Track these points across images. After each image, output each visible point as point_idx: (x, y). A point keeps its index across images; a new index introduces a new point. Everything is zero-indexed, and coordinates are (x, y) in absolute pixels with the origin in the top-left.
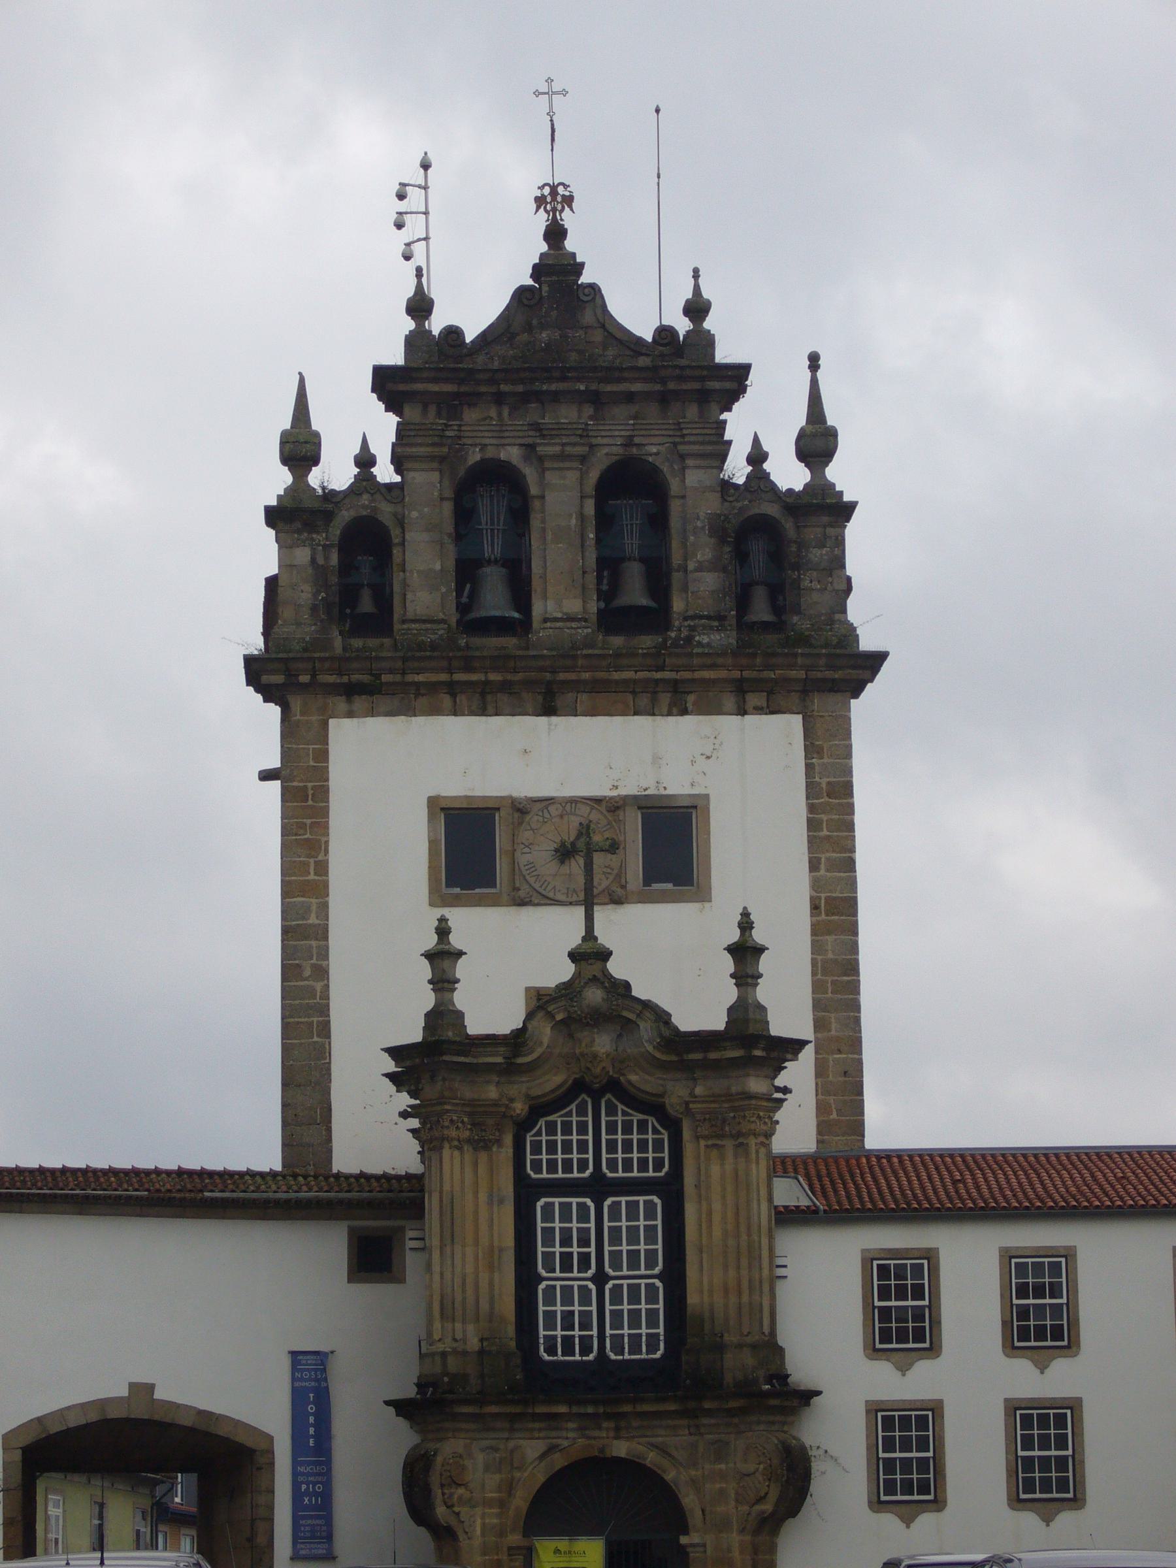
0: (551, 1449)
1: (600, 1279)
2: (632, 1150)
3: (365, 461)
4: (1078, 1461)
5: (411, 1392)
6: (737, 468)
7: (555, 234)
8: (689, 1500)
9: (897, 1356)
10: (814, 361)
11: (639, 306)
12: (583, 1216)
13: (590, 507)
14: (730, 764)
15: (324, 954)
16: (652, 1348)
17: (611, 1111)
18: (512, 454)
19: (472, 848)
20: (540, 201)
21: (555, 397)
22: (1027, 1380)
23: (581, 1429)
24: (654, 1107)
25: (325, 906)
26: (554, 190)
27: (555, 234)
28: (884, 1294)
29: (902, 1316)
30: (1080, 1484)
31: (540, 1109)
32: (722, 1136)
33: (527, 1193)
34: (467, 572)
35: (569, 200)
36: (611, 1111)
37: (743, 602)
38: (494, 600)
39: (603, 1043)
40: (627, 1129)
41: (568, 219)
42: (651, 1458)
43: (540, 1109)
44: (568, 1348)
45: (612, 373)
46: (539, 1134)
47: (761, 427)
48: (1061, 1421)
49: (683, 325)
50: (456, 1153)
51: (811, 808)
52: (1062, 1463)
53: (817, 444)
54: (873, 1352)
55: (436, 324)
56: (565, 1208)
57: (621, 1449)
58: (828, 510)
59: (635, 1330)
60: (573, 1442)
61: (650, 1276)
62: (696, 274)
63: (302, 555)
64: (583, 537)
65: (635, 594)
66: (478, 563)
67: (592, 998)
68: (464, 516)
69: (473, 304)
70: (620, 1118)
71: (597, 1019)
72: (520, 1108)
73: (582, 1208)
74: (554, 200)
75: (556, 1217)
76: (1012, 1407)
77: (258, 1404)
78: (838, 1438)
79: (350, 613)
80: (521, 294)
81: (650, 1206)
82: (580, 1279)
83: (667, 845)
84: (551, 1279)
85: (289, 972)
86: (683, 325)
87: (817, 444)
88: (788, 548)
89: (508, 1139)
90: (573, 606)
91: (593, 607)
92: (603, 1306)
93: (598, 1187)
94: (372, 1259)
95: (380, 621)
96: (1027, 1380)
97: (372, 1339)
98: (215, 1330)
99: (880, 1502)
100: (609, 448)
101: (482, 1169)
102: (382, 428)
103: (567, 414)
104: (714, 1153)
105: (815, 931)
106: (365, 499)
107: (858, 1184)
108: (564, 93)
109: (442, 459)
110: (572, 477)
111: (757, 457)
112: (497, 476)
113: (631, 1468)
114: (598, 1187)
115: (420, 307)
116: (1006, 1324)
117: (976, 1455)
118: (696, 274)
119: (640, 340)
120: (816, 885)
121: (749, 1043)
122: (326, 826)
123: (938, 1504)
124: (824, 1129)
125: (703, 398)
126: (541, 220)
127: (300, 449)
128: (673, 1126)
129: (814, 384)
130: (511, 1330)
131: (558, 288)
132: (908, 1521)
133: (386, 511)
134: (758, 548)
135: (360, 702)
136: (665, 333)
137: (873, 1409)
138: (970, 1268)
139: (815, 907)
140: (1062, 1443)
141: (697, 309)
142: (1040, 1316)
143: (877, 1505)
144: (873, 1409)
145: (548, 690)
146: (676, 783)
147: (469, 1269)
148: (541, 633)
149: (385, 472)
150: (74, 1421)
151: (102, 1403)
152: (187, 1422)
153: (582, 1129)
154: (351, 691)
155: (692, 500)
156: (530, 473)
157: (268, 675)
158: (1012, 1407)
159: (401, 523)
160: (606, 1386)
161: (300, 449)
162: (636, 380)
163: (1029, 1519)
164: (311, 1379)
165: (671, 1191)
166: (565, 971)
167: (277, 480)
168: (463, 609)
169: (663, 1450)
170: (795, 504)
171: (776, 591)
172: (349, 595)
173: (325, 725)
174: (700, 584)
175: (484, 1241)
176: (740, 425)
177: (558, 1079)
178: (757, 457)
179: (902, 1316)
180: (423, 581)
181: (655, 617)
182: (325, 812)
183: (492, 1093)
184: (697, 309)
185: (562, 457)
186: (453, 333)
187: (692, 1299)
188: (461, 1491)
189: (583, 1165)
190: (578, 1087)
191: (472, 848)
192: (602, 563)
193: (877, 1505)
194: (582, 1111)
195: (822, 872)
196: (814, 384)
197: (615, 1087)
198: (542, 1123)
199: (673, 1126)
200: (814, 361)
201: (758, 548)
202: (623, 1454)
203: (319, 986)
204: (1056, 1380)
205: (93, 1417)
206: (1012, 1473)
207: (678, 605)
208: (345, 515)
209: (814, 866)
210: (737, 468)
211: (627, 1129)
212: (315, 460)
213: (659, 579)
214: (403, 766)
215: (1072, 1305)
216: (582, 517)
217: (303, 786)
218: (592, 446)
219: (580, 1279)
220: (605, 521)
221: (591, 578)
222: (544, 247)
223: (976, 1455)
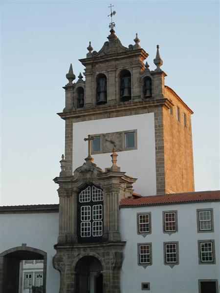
0: (79, 254)
3: (81, 77)
7: (112, 31)
9: (143, 234)
10: (158, 47)
12: (89, 210)
14: (142, 123)
16: (100, 234)
17: (94, 189)
18: (103, 72)
19: (96, 142)
20: (110, 26)
23: (84, 250)
25: (72, 157)
26: (112, 23)
27: (112, 31)
28: (141, 222)
29: (144, 226)
32: (109, 192)
33: (79, 205)
35: (114, 25)
36: (94, 189)
39: (88, 176)
40: (96, 192)
41: (114, 29)
42: (97, 256)
43: (81, 189)
45: (118, 54)
46: (81, 194)
48: (174, 246)
49: (134, 44)
50: (63, 199)
51: (156, 130)
52: (175, 255)
53: (158, 62)
54: (139, 233)
55: (92, 52)
56: (86, 208)
57: (91, 254)
58: (160, 73)
60: (83, 254)
62: (137, 34)
63: (69, 95)
64: (116, 86)
69: (97, 48)
70: (95, 190)
71: (87, 171)
73: (89, 208)
74: (112, 25)
75: (87, 210)
76: (165, 244)
79: (80, 103)
84: (84, 222)
86: (134, 44)
90: (114, 98)
91: (118, 97)
93: (91, 204)
95: (82, 105)
99: (201, 262)
100: (120, 68)
101: (68, 200)
104: (108, 195)
105: (156, 153)
106: (80, 84)
108: (113, 6)
109: (92, 74)
110: (114, 74)
112: (102, 77)
113: (93, 258)
115: (90, 49)
116: (164, 227)
117: (158, 254)
118: (137, 34)
119: (126, 48)
120: (156, 145)
122: (72, 143)
123: (151, 264)
124: (158, 191)
126: (110, 29)
127: (71, 76)
129: (158, 50)
132: (145, 268)
136: (130, 46)
137: (139, 245)
138: (157, 215)
139: (156, 149)
140: (174, 251)
141: (137, 41)
142: (170, 224)
143: (139, 264)
144: (139, 245)
145: (108, 113)
146: (130, 128)
147: (66, 220)
149: (84, 79)
150: (12, 251)
152: (31, 250)
153: (89, 193)
155: (135, 75)
156: (106, 75)
158: (165, 244)
159: (85, 86)
162: (123, 55)
163: (168, 267)
167: (67, 82)
168: (97, 101)
169: (98, 254)
170: (153, 73)
171: (151, 90)
173: (72, 124)
175: (68, 215)
177: (82, 183)
179: (144, 226)
180: (89, 97)
181: (128, 98)
182: (72, 140)
183: (70, 187)
184: (137, 41)
185: (111, 71)
186: (95, 52)
188: (61, 263)
189: (89, 199)
193: (139, 264)
194: (89, 189)
195: (158, 142)
196: (158, 50)
197: (92, 184)
198: (82, 192)
200: (158, 47)
201: (148, 82)
202: (92, 255)
203: (70, 171)
205: (15, 250)
207: (132, 95)
208: (77, 87)
209: (156, 141)
211: (96, 192)
215: (177, 222)
216: (115, 81)
218: (117, 68)
219: (88, 221)
222: (110, 33)
223: (158, 254)
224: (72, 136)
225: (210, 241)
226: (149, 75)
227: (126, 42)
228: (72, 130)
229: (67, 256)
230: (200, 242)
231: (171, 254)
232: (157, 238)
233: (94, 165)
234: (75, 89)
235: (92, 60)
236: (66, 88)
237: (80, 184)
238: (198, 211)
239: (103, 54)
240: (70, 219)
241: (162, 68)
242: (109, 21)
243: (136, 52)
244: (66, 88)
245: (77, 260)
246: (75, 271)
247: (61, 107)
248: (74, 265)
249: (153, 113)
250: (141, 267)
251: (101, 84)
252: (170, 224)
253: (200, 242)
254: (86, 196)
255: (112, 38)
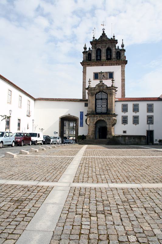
0: (97, 119)
1: (102, 106)
2: (104, 96)
3: (90, 49)
4: (138, 120)
5: (86, 114)
6: (117, 48)
7: (104, 32)
8: (107, 123)
10: (123, 40)
11: (109, 36)
13: (106, 51)
14: (116, 70)
15: (86, 84)
17: (103, 93)
18: (100, 47)
19: (96, 76)
21: (103, 43)
22: (135, 114)
24: (106, 93)
27: (104, 32)
29: (125, 109)
30: (139, 122)
31: (97, 93)
33: (96, 99)
34: (97, 56)
36: (103, 93)
37: (117, 58)
38: (99, 58)
41: (104, 31)
42: (105, 120)
43: (97, 93)
44: (99, 111)
45: (107, 41)
47: (119, 45)
48: (137, 117)
49: (113, 38)
53: (123, 46)
54: (122, 112)
55: (95, 39)
57: (102, 119)
59: (104, 110)
60: (99, 118)
61: (105, 106)
63: (85, 55)
65: (109, 57)
66: (98, 56)
67: (101, 85)
68: (97, 52)
69: (97, 37)
71: (101, 86)
72: (95, 93)
74: (104, 29)
76: (133, 116)
77: (78, 116)
78: (119, 119)
79: (89, 59)
80: (101, 36)
81: (105, 101)
82: (100, 106)
83: (111, 75)
84: (98, 106)
85: (83, 85)
86: (113, 38)
87: (123, 46)
88: (120, 53)
89: (94, 95)
90: (104, 58)
92: (101, 108)
93: (102, 99)
94: (86, 105)
96: (135, 114)
97: (85, 110)
98: (75, 110)
100: (107, 47)
102: (91, 46)
103: (104, 44)
107: (123, 99)
110: (104, 49)
111: (118, 47)
113: (103, 120)
114: (102, 99)
115: (94, 38)
116: (133, 110)
117: (130, 120)
121: (113, 88)
123: (127, 124)
124: (122, 96)
125: (114, 42)
126: (103, 31)
127: (85, 48)
128: (107, 94)
130: (94, 110)
131: (104, 34)
133: (91, 52)
134: (118, 54)
135: (89, 66)
136: (111, 38)
137: (122, 116)
138: (130, 105)
139: (122, 80)
141: (114, 37)
142: (136, 109)
143: (122, 124)
144: (122, 116)
146: (111, 71)
148: (102, 60)
150: (64, 116)
151: (66, 115)
152: (72, 116)
154: (88, 65)
156: (101, 49)
157: (82, 64)
158: (133, 116)
159: (92, 52)
160: (101, 114)
161: (85, 48)
163: (134, 125)
164: (82, 113)
165: (107, 99)
166: (99, 82)
168: (96, 59)
169: (105, 119)
170: (121, 50)
172: (88, 58)
174: (114, 55)
176: (117, 45)
178: (118, 47)
179: (125, 109)
180: (94, 56)
184: (114, 37)
186: (96, 39)
187: (108, 107)
190: (100, 91)
191: (96, 76)
192: (106, 55)
193: (122, 124)
199: (107, 94)
200: (123, 40)
201: (118, 54)
204: (137, 114)
205: (66, 116)
206: (133, 121)
207: (112, 58)
208: (88, 52)
209: (122, 77)
210: (117, 48)
212: (86, 49)
213: (111, 56)
214: (92, 70)
217: (84, 72)
220: (107, 52)
221: (106, 56)
223: (130, 120)
224: (86, 72)
225: (152, 116)
226: (119, 50)
227: (109, 36)
228: (86, 70)
229: (91, 119)
230: (147, 116)
231: (136, 120)
232: (130, 114)
233: (103, 84)
234: (87, 54)
235: (94, 43)
236: (83, 53)
237: (98, 91)
238: (147, 104)
239: (100, 40)
240: (93, 104)
241: (124, 48)
242: (102, 27)
243: (114, 41)
244: (83, 53)
245: (96, 121)
246: (95, 125)
247: (81, 60)
248: (95, 123)
249: (121, 66)
250: (123, 125)
251: (98, 53)
252: (136, 109)
253: (147, 116)
254: (99, 96)
255: (104, 34)
